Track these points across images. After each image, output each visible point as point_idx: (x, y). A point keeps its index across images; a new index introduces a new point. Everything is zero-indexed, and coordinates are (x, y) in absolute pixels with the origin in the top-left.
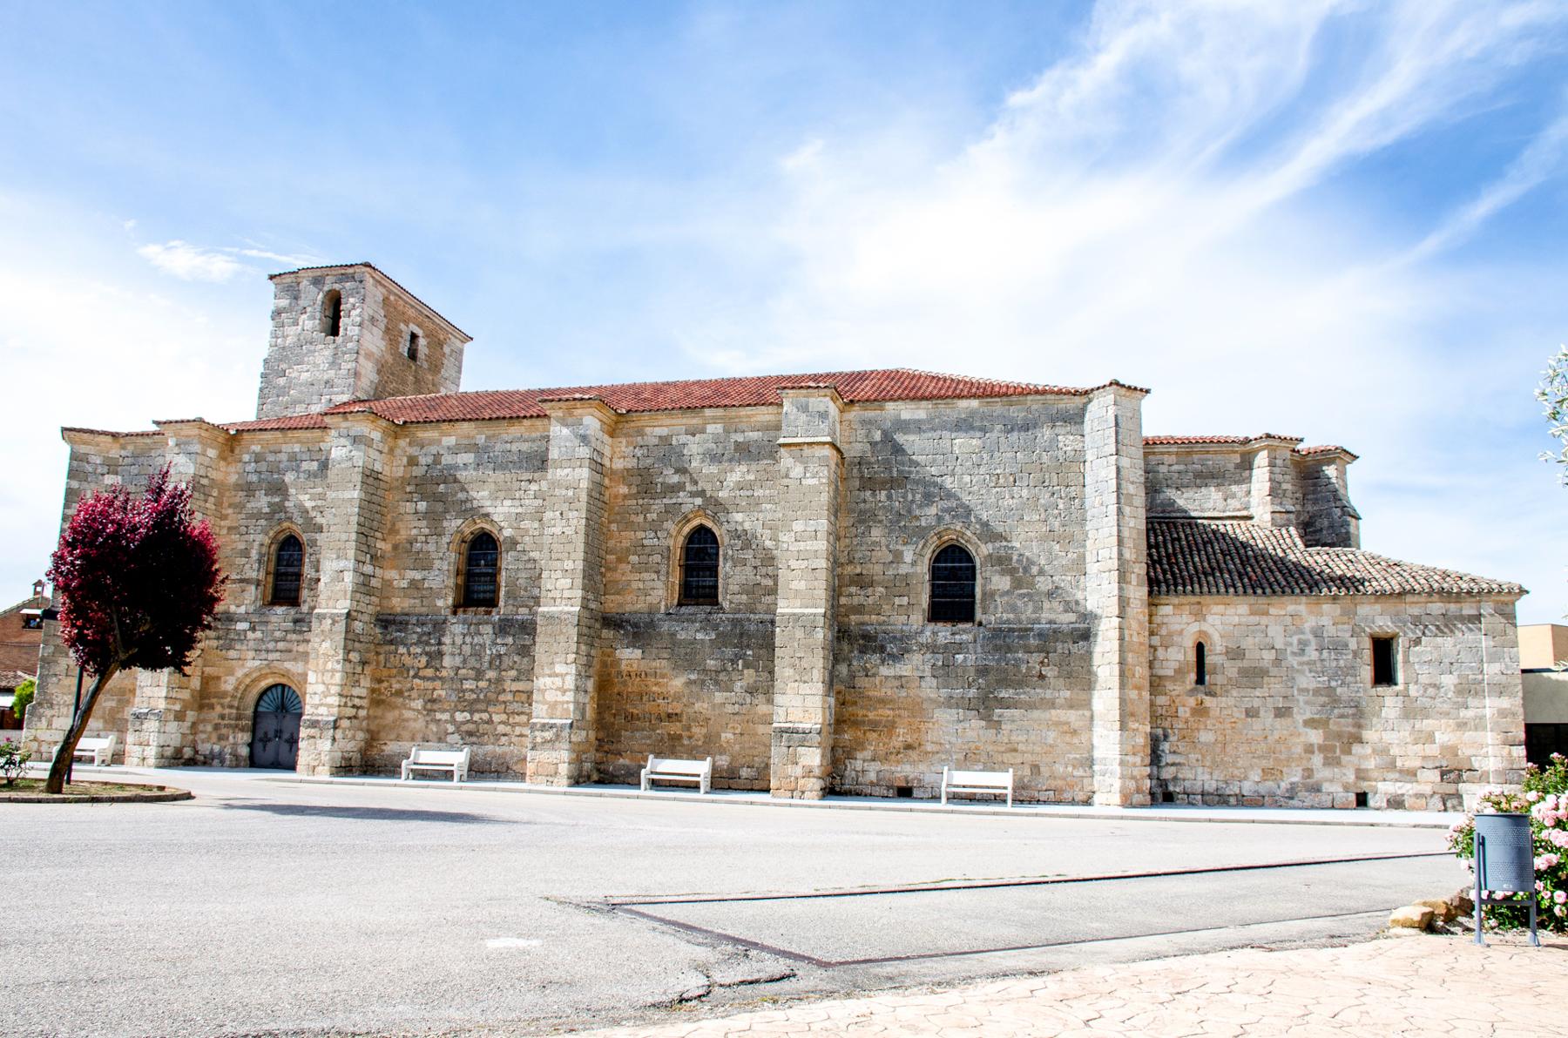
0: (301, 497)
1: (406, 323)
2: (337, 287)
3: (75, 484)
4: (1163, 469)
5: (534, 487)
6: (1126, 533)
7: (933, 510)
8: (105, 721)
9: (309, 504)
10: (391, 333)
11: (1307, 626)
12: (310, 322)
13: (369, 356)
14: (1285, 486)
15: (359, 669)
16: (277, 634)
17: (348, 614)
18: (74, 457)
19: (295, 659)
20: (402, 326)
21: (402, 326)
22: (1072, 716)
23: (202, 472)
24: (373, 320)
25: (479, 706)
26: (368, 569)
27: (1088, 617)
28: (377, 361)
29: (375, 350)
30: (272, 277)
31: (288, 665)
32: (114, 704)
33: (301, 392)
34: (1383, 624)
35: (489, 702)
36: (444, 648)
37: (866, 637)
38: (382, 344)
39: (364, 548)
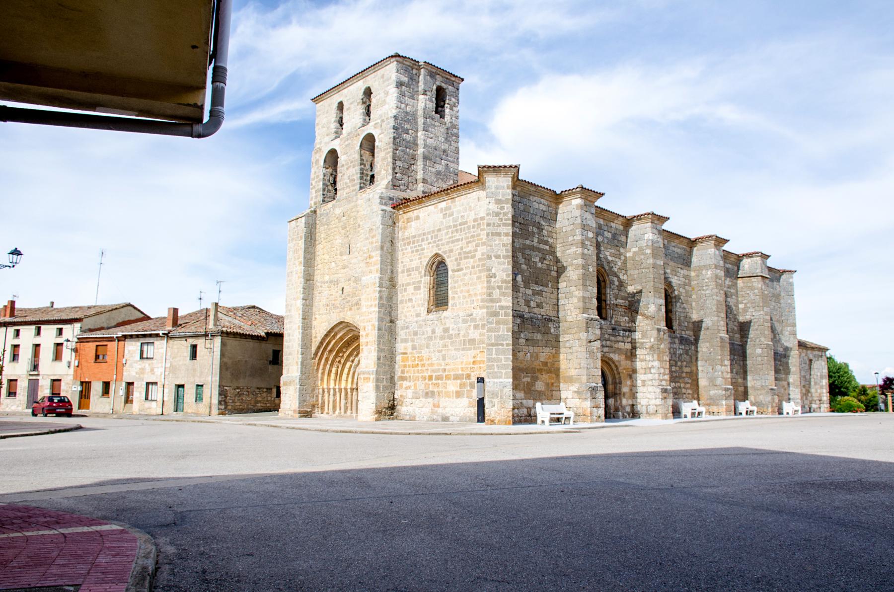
0: (608, 254)
2: (443, 85)
5: (682, 272)
8: (525, 393)
9: (610, 258)
12: (424, 102)
16: (606, 336)
19: (614, 352)
22: (785, 383)
25: (677, 380)
27: (787, 349)
31: (612, 355)
32: (529, 379)
33: (429, 152)
34: (811, 357)
35: (680, 377)
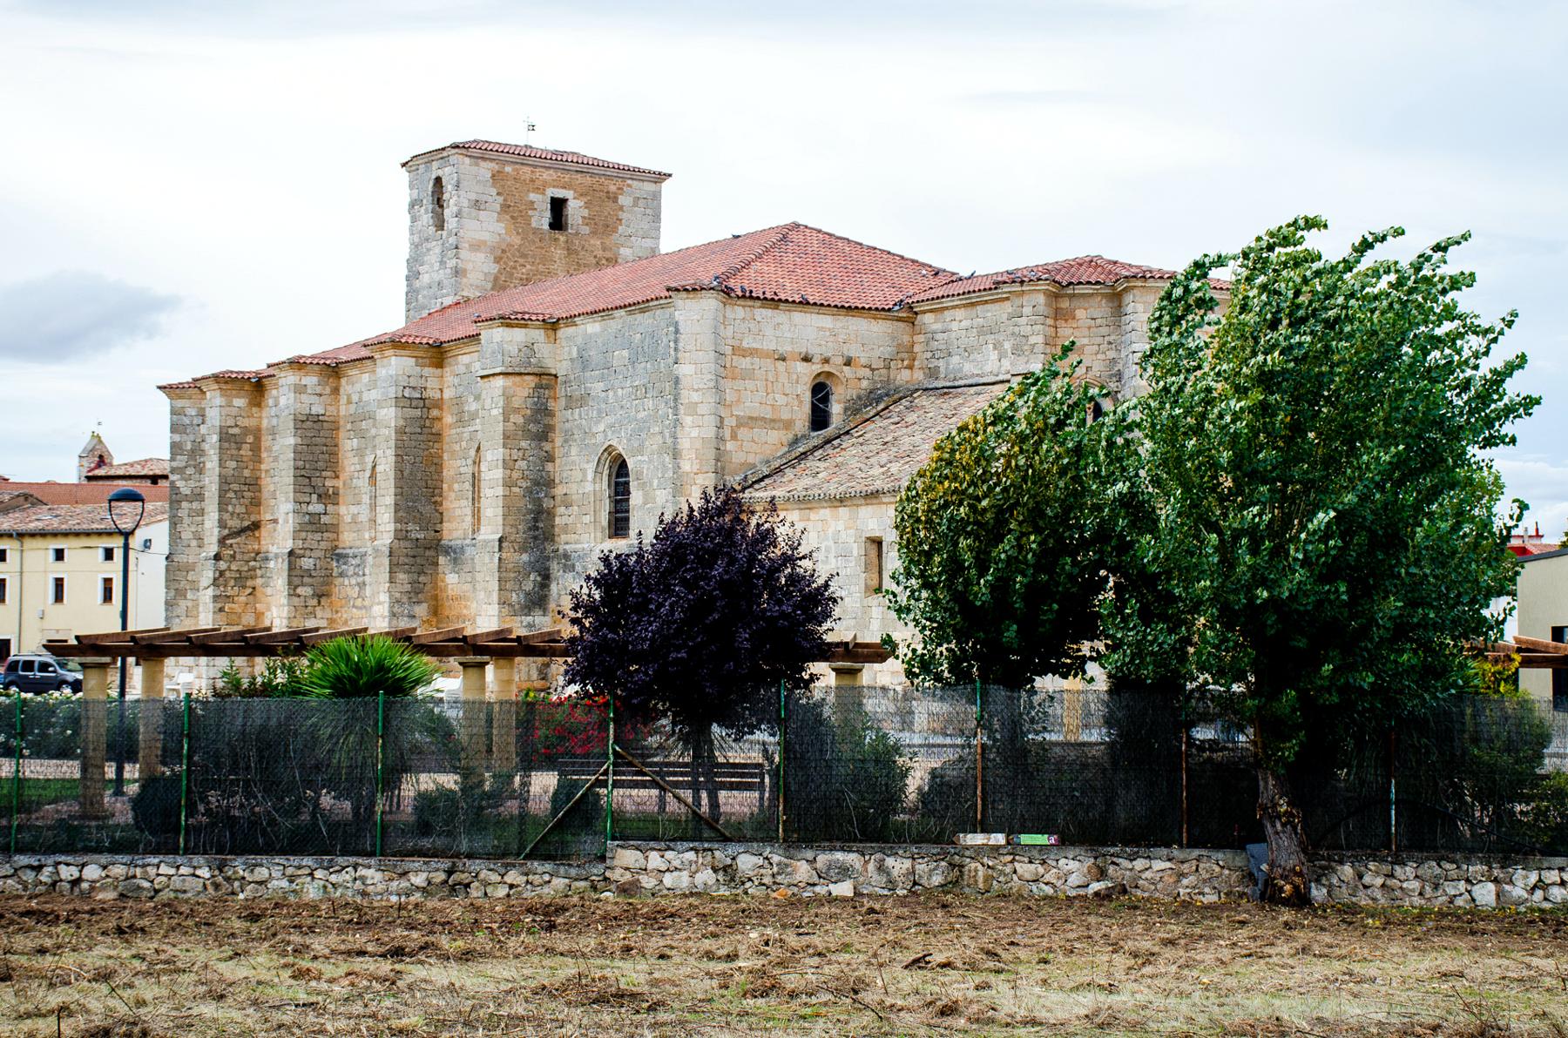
1: (540, 190)
3: (177, 438)
4: (954, 326)
6: (684, 444)
7: (601, 427)
10: (512, 211)
11: (831, 531)
13: (476, 246)
14: (1033, 340)
15: (315, 602)
17: (291, 553)
18: (173, 412)
20: (532, 196)
21: (532, 196)
23: (230, 422)
24: (477, 205)
26: (316, 507)
28: (493, 249)
29: (486, 236)
30: (404, 165)
36: (367, 579)
37: (566, 556)
38: (500, 228)
39: (308, 490)
